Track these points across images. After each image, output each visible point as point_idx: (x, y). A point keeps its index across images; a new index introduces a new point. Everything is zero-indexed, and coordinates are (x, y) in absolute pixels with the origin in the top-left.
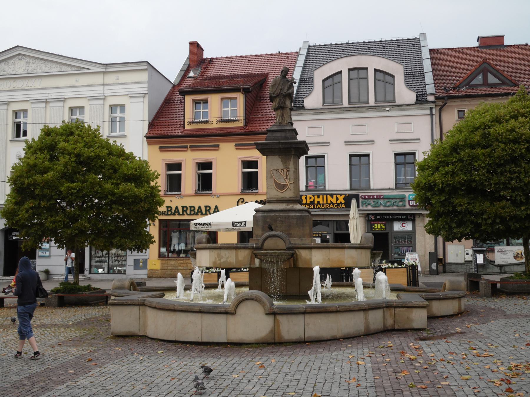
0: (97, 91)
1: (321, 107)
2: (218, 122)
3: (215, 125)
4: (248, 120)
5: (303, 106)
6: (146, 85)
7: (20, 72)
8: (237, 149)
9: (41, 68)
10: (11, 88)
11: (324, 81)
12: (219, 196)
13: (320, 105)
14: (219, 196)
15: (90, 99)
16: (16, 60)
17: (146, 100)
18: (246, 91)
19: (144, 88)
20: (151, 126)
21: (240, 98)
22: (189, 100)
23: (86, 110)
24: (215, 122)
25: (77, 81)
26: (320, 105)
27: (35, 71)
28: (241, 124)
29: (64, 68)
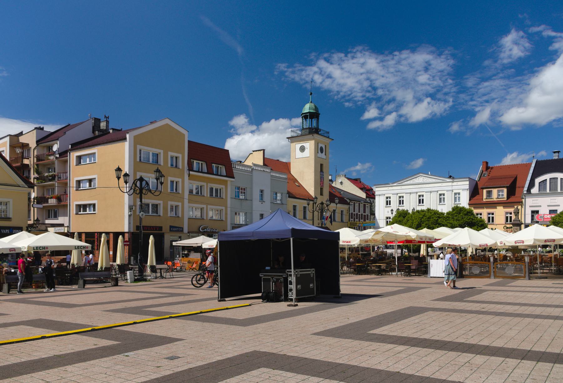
0: (450, 188)
1: (538, 192)
2: (496, 198)
3: (495, 200)
4: (508, 197)
5: (530, 192)
6: (468, 186)
7: (421, 182)
8: (504, 208)
9: (429, 180)
10: (418, 187)
11: (539, 183)
12: (497, 225)
13: (537, 192)
14: (497, 225)
15: (447, 191)
16: (419, 177)
17: (468, 191)
18: (507, 187)
19: (467, 187)
20: (470, 200)
21: (505, 190)
22: (485, 191)
23: (446, 195)
24: (495, 199)
25: (442, 185)
26: (537, 192)
27: (426, 181)
28: (506, 199)
29: (437, 180)
